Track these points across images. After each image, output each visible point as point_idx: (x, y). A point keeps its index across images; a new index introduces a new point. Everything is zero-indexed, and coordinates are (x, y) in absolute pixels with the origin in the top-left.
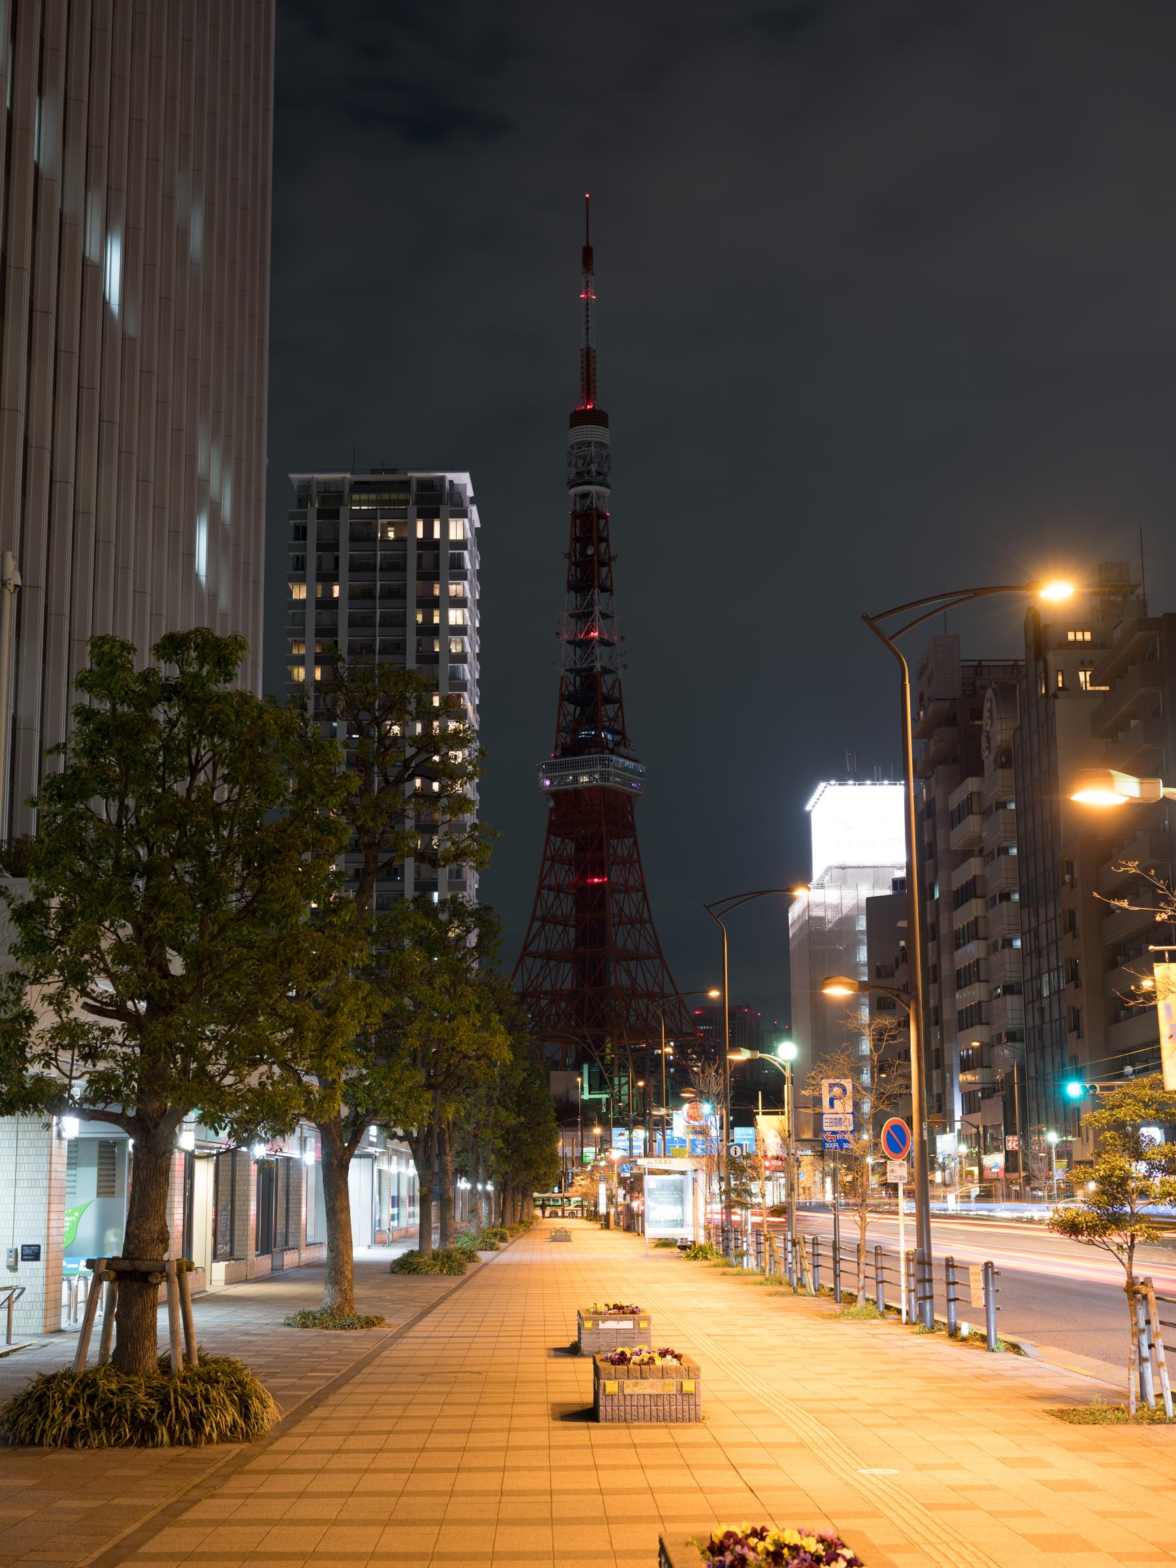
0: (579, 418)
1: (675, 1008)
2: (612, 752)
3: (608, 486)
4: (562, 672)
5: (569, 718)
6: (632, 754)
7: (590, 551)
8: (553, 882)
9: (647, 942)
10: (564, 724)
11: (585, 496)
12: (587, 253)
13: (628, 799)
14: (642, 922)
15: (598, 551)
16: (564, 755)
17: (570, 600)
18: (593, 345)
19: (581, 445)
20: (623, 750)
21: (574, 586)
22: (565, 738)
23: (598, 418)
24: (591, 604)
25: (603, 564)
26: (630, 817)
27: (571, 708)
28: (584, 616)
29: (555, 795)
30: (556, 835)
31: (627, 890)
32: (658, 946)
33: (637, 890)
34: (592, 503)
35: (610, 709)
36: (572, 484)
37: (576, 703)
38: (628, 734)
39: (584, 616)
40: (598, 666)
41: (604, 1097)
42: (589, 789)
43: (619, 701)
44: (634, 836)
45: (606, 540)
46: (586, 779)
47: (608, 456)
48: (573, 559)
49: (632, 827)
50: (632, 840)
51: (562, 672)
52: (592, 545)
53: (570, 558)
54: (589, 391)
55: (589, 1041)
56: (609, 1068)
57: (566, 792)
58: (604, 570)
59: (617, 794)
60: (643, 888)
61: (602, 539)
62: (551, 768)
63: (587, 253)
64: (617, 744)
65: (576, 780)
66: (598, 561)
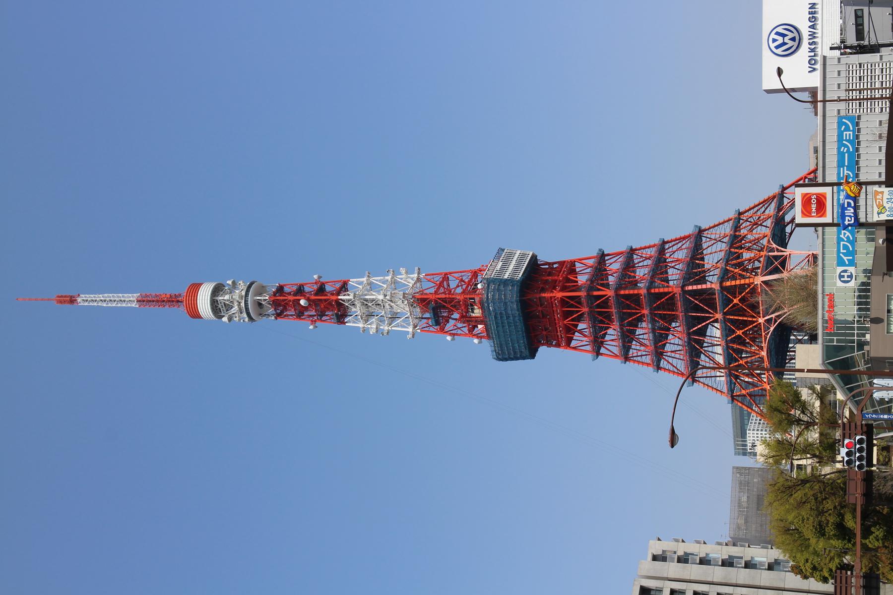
1: (747, 221)
5: (460, 325)
9: (678, 250)
10: (466, 330)
26: (555, 266)
27: (452, 322)
30: (571, 339)
32: (684, 238)
34: (265, 300)
43: (446, 277)
44: (573, 263)
48: (315, 318)
50: (577, 264)
52: (300, 300)
53: (315, 321)
55: (773, 316)
66: (316, 294)
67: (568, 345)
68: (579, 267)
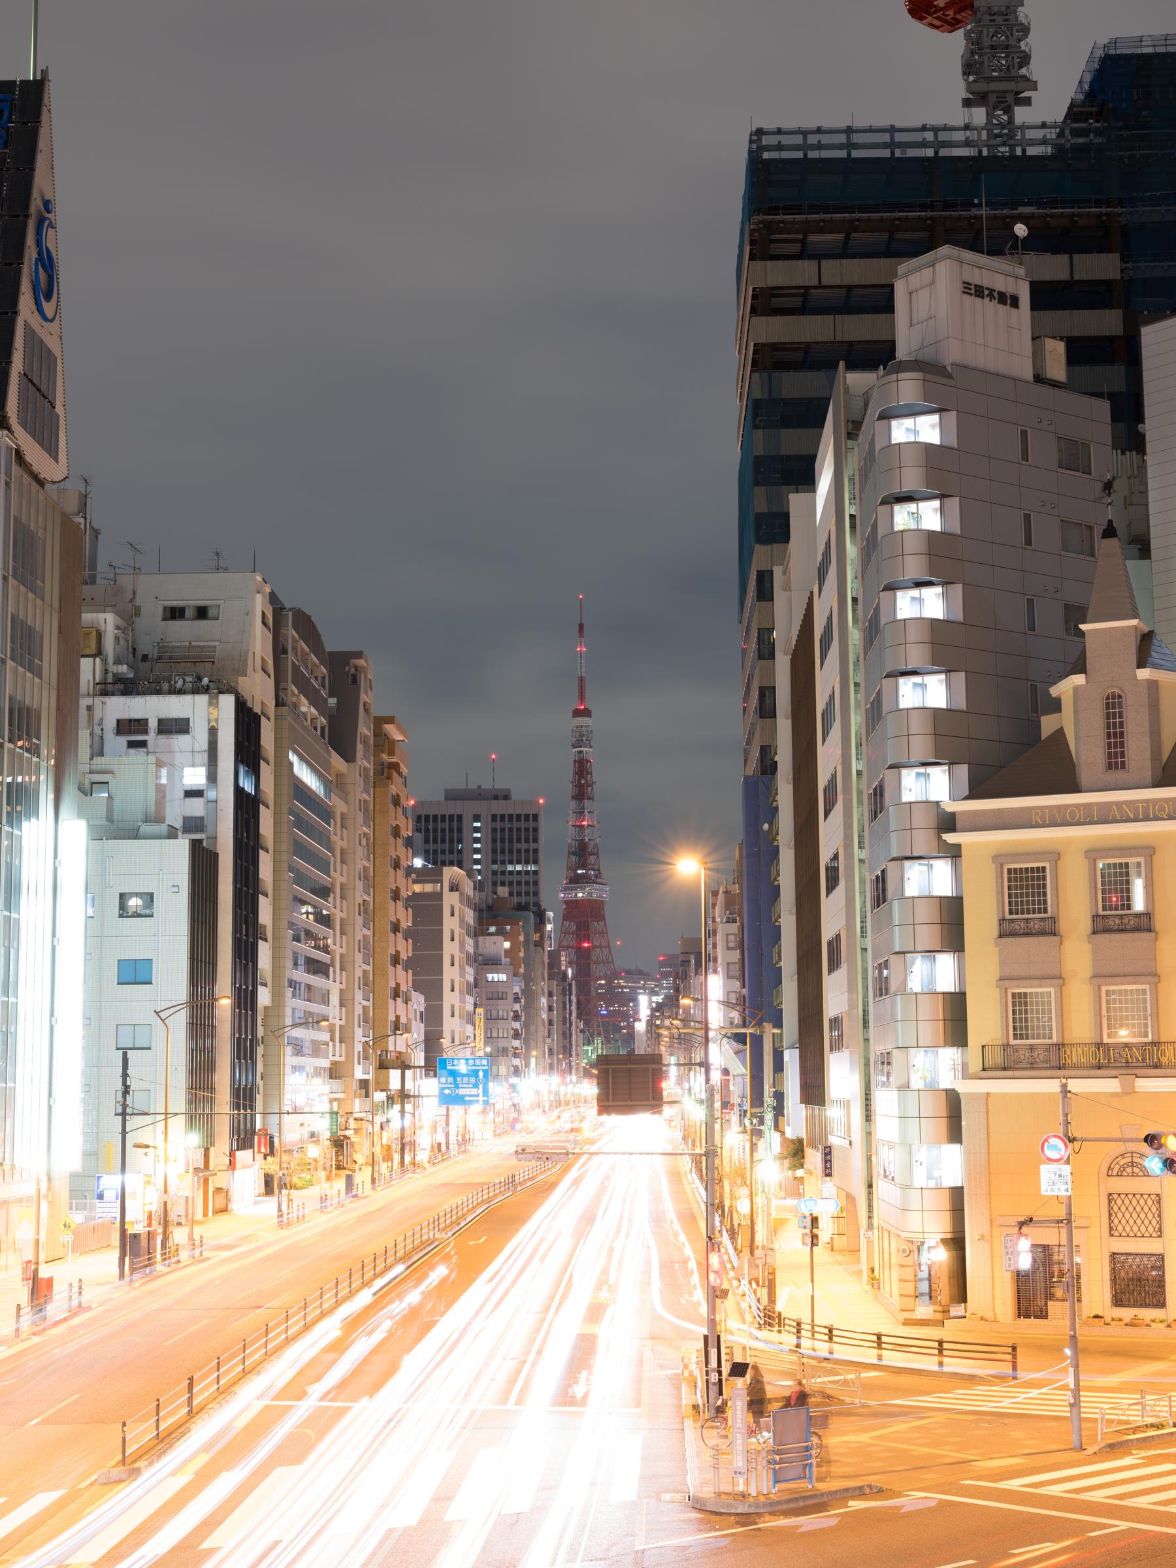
0: (577, 713)
2: (594, 883)
3: (591, 747)
4: (569, 841)
6: (603, 881)
7: (583, 782)
8: (565, 944)
11: (580, 752)
12: (581, 626)
13: (602, 902)
14: (608, 962)
15: (586, 780)
16: (570, 883)
17: (573, 804)
18: (583, 674)
19: (577, 727)
20: (599, 880)
21: (574, 798)
22: (571, 873)
23: (586, 713)
24: (583, 808)
25: (588, 786)
27: (573, 858)
28: (580, 813)
29: (566, 902)
31: (600, 947)
33: (605, 947)
35: (592, 859)
36: (574, 746)
37: (576, 855)
38: (601, 871)
39: (580, 813)
40: (587, 840)
41: (590, 1049)
42: (583, 900)
43: (597, 854)
45: (591, 773)
46: (580, 895)
47: (591, 732)
49: (604, 918)
51: (569, 841)
54: (582, 698)
56: (592, 1036)
57: (571, 901)
58: (590, 789)
59: (596, 901)
60: (609, 946)
61: (588, 774)
62: (565, 889)
63: (581, 626)
64: (596, 876)
65: (576, 895)
67: (563, 920)
68: (602, 923)
